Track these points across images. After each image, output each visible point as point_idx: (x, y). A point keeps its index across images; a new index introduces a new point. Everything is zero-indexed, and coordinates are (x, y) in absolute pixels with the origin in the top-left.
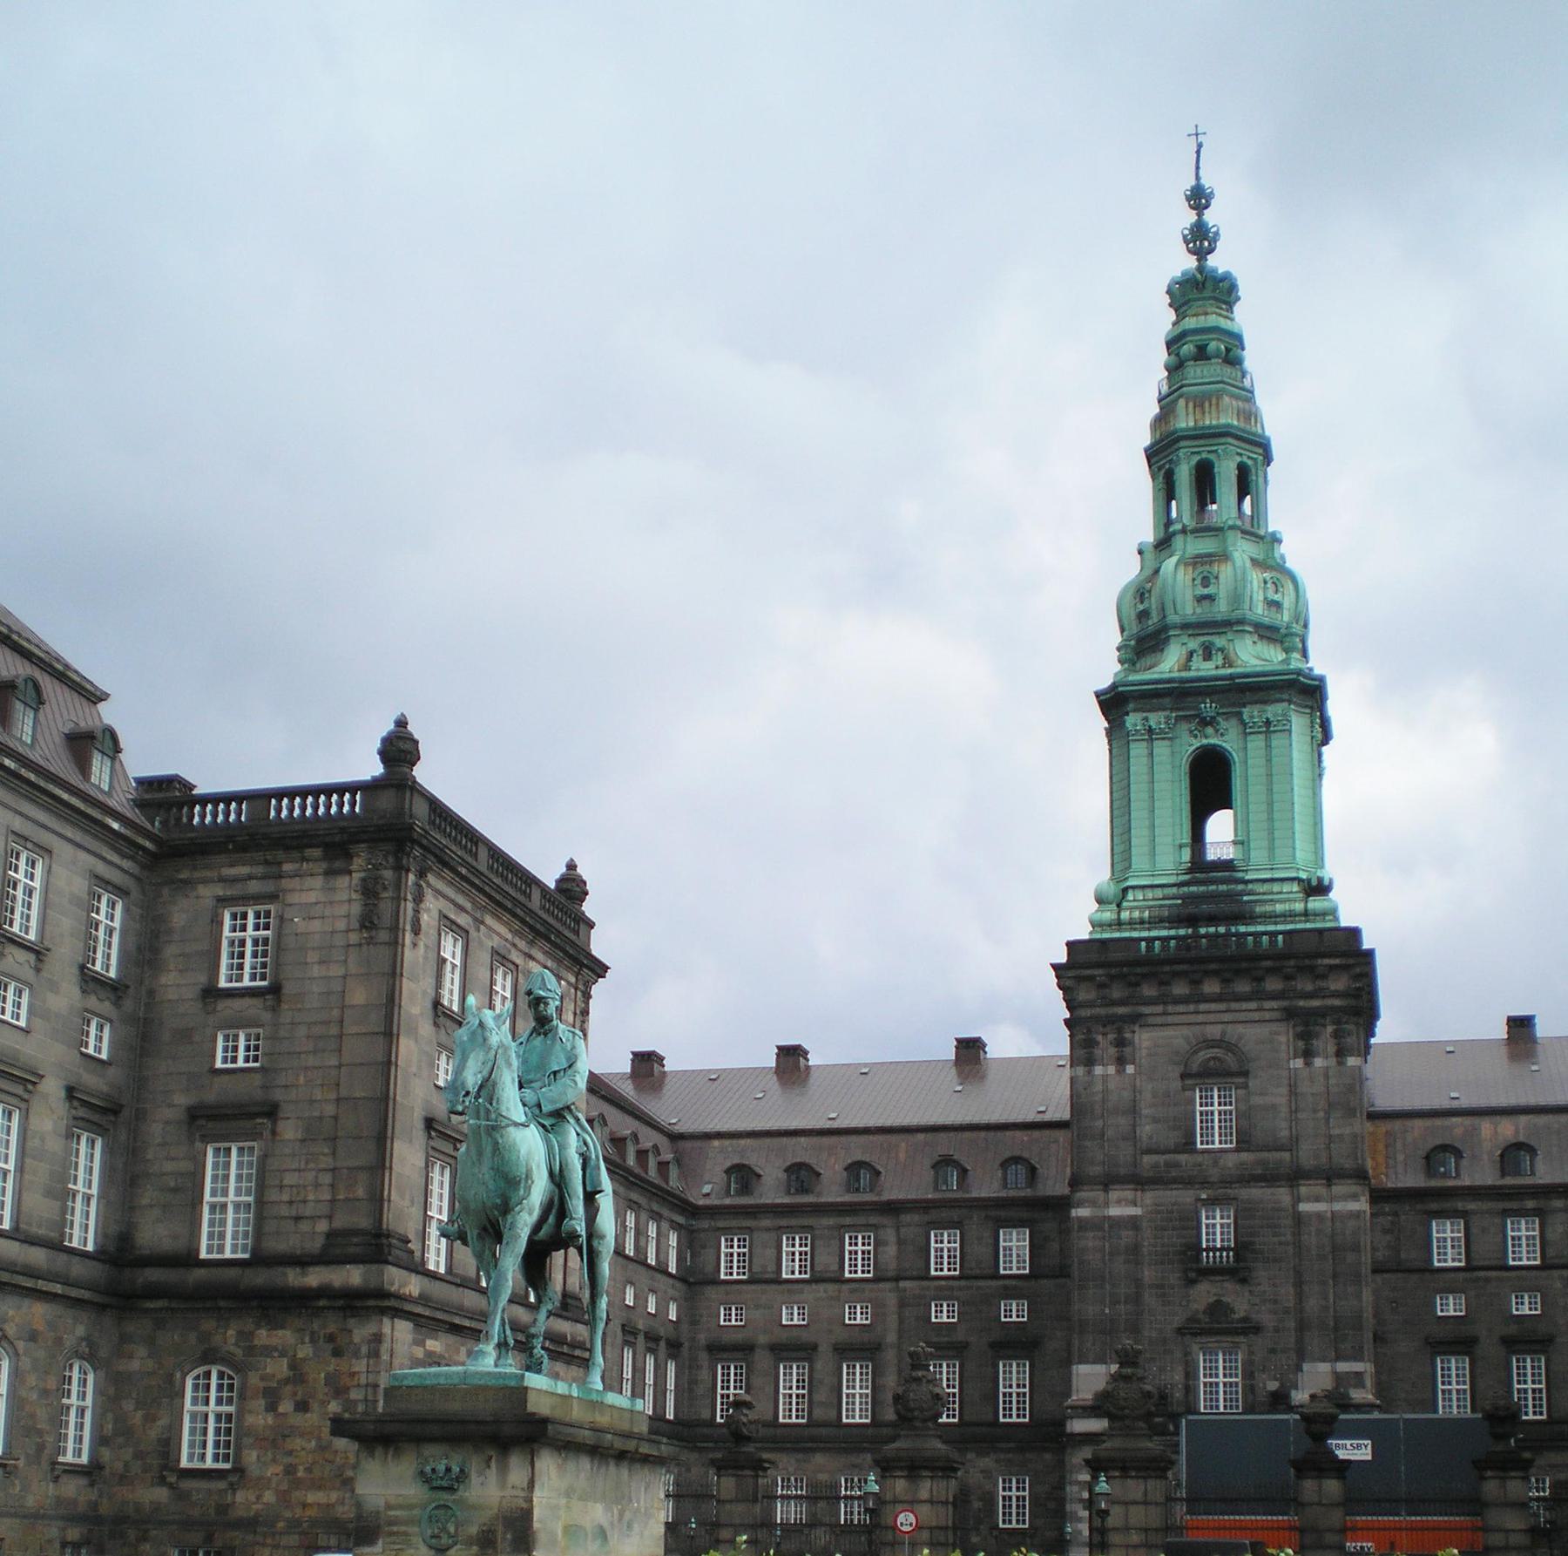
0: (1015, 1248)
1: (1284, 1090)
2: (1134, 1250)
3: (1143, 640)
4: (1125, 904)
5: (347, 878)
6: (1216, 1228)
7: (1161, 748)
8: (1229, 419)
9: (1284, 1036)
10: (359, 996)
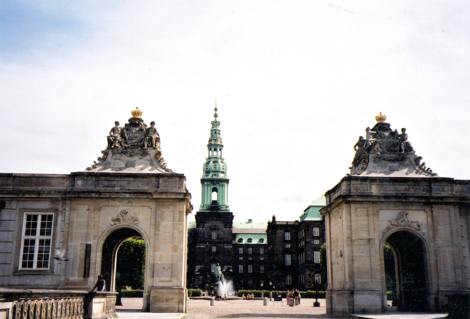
3: (207, 172)
6: (214, 249)
7: (209, 187)
8: (219, 143)
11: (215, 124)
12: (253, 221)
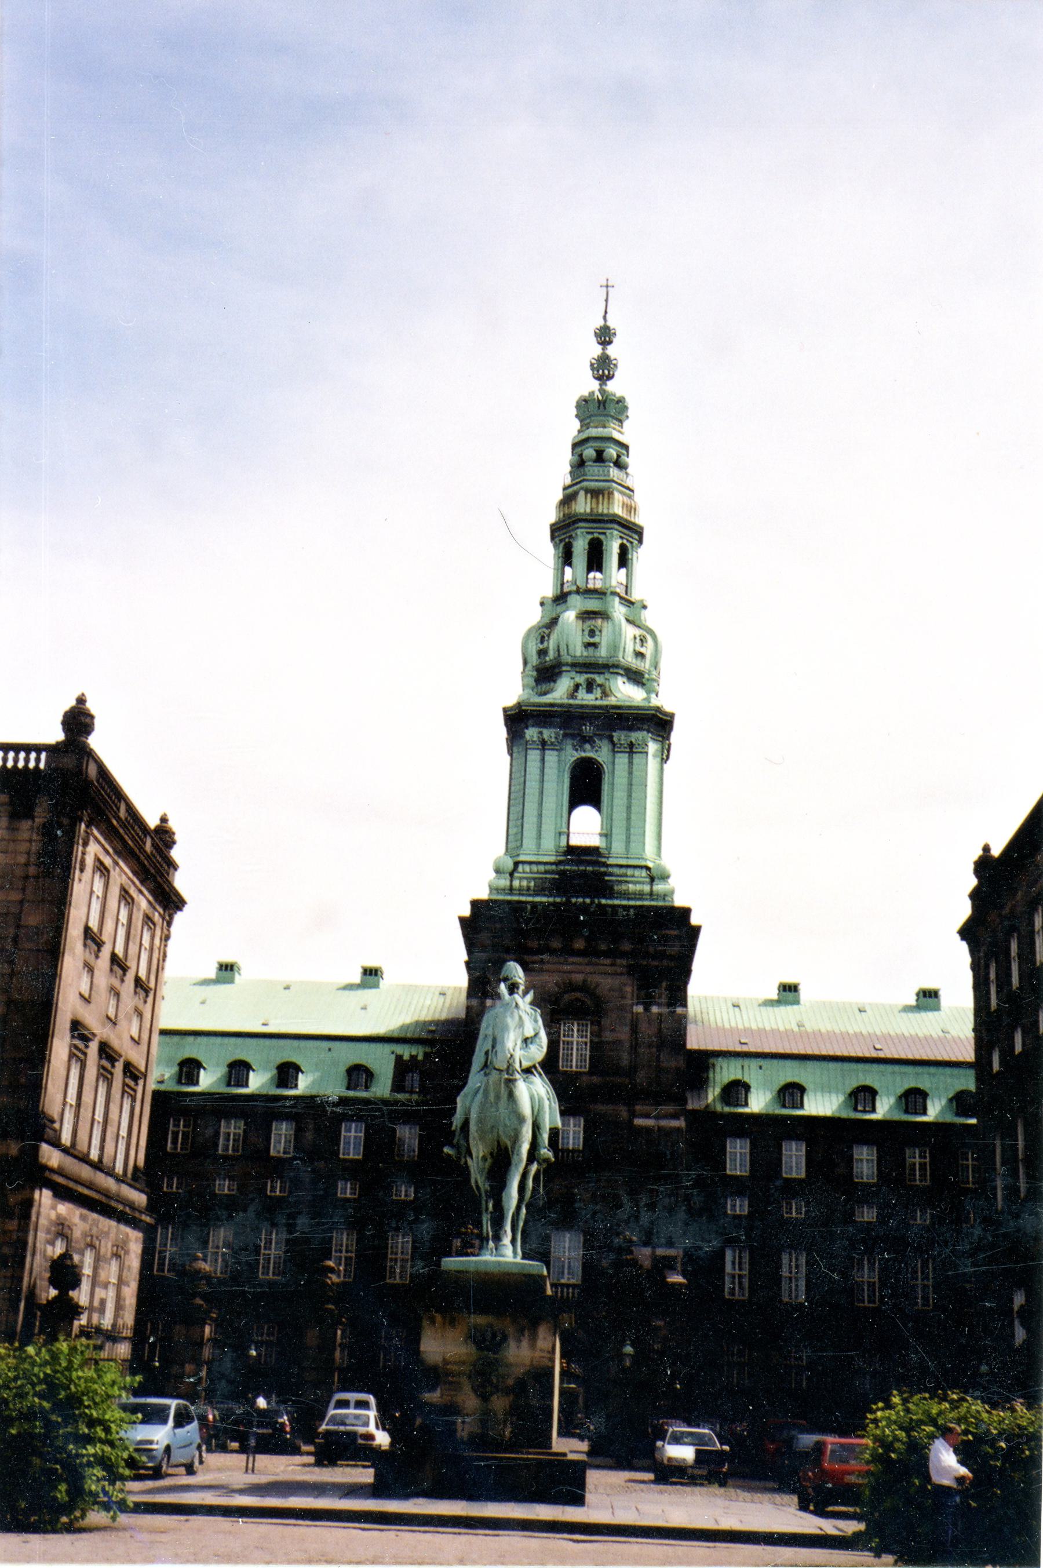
0: (408, 1135)
1: (627, 1029)
4: (516, 875)
5: (30, 823)
7: (551, 757)
8: (618, 510)
11: (600, 410)
12: (804, 993)
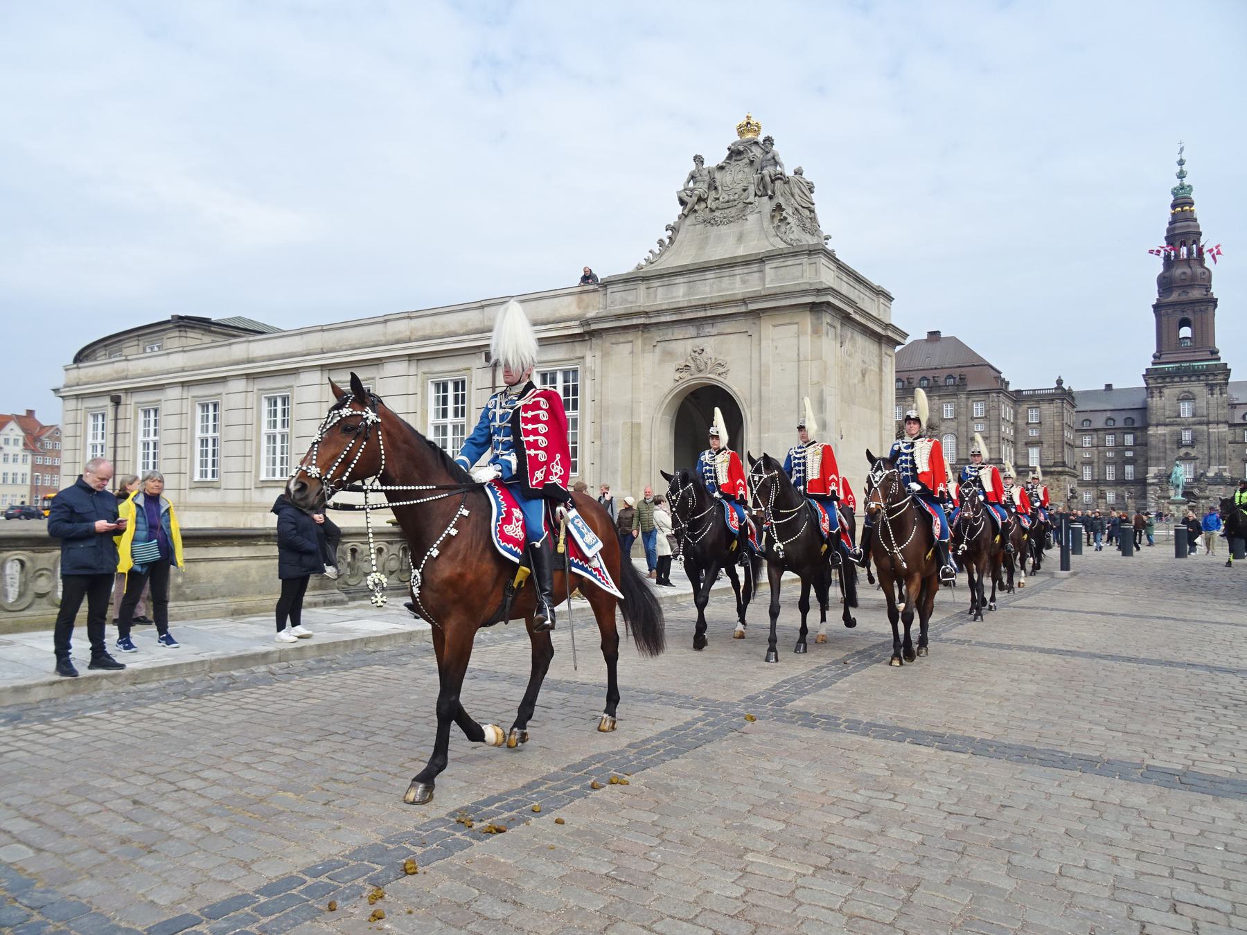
0: (1129, 440)
2: (1164, 441)
6: (1186, 436)
9: (1206, 390)
10: (1057, 424)
